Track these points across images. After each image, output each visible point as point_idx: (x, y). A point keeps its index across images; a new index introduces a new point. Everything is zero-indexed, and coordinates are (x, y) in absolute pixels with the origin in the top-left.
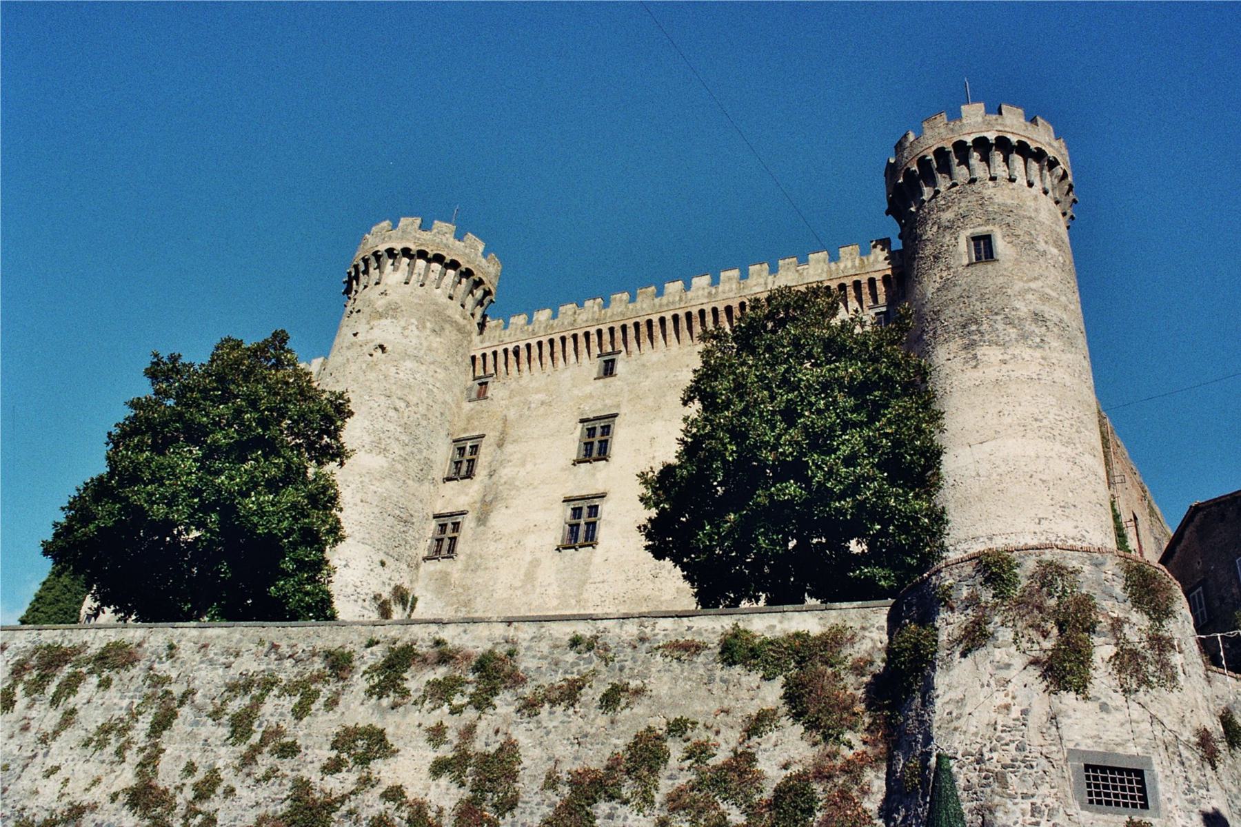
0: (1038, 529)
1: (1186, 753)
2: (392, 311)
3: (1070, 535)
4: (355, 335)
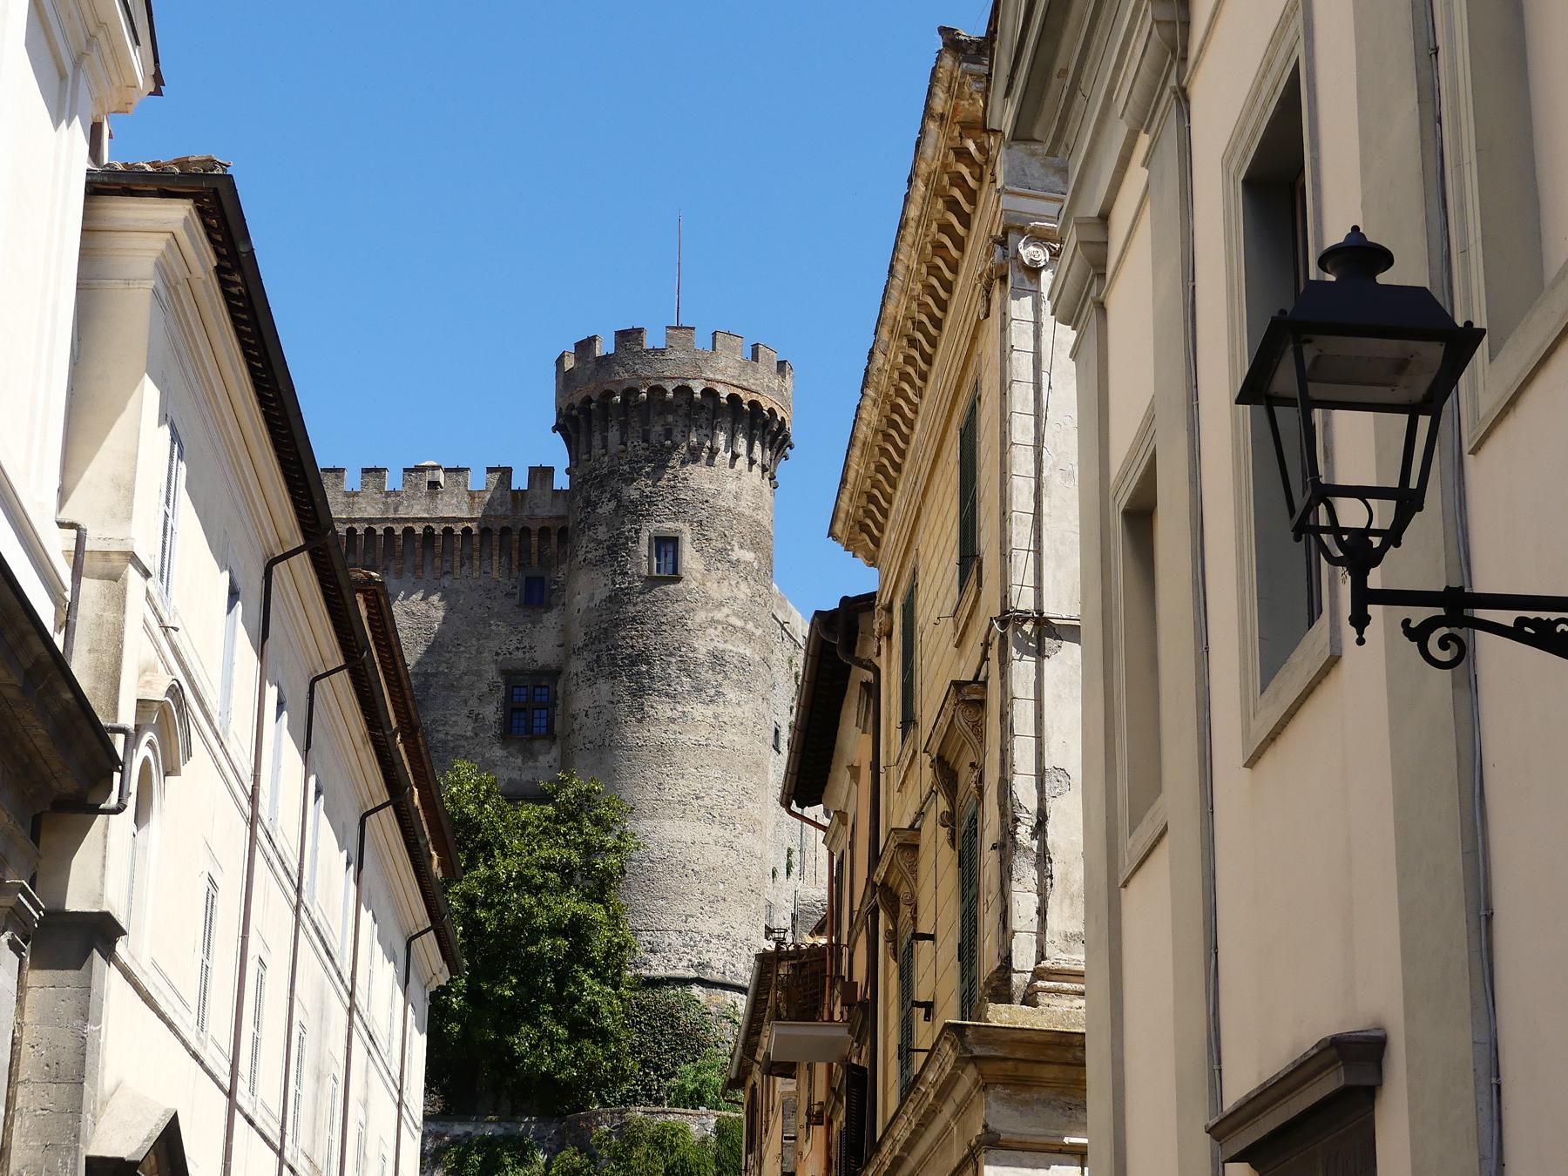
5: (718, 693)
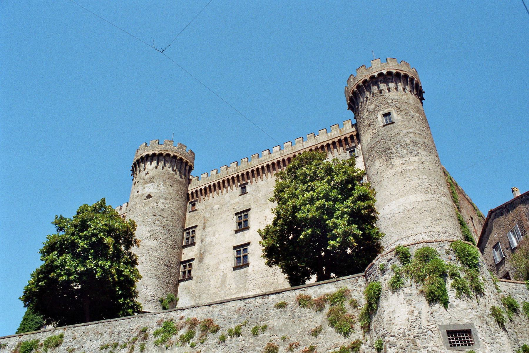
0: (426, 231)
1: (488, 319)
2: (152, 180)
4: (138, 192)
5: (418, 153)
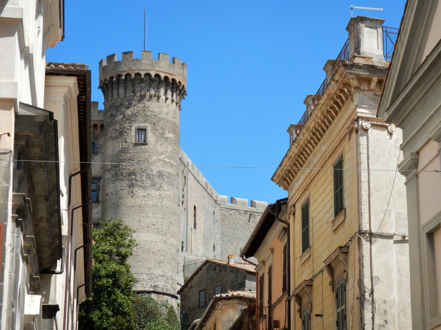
0: (148, 272)
3: (160, 275)
